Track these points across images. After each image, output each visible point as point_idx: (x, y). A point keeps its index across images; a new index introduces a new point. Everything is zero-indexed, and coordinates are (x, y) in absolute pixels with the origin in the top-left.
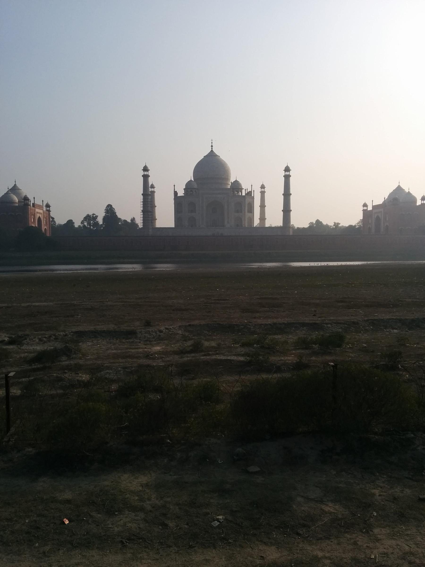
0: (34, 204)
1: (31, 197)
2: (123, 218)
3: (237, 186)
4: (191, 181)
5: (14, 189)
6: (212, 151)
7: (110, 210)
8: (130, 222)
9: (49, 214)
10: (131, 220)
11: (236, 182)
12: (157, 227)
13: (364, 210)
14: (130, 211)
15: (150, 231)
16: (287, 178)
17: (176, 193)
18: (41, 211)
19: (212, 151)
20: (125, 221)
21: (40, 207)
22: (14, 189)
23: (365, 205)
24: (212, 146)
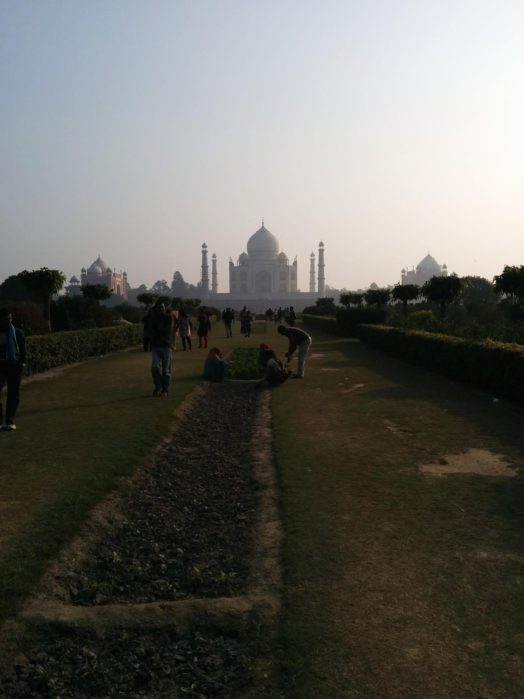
0: (114, 274)
1: (112, 269)
2: (190, 283)
3: (283, 258)
4: (244, 254)
5: (98, 262)
6: (263, 227)
7: (178, 277)
8: (197, 286)
9: (126, 281)
10: (198, 284)
11: (282, 253)
12: (218, 292)
13: (402, 276)
14: (193, 278)
15: (208, 296)
16: (321, 251)
17: (231, 264)
18: (120, 280)
19: (263, 227)
20: (192, 286)
21: (119, 276)
22: (98, 262)
23: (403, 271)
24: (263, 223)
